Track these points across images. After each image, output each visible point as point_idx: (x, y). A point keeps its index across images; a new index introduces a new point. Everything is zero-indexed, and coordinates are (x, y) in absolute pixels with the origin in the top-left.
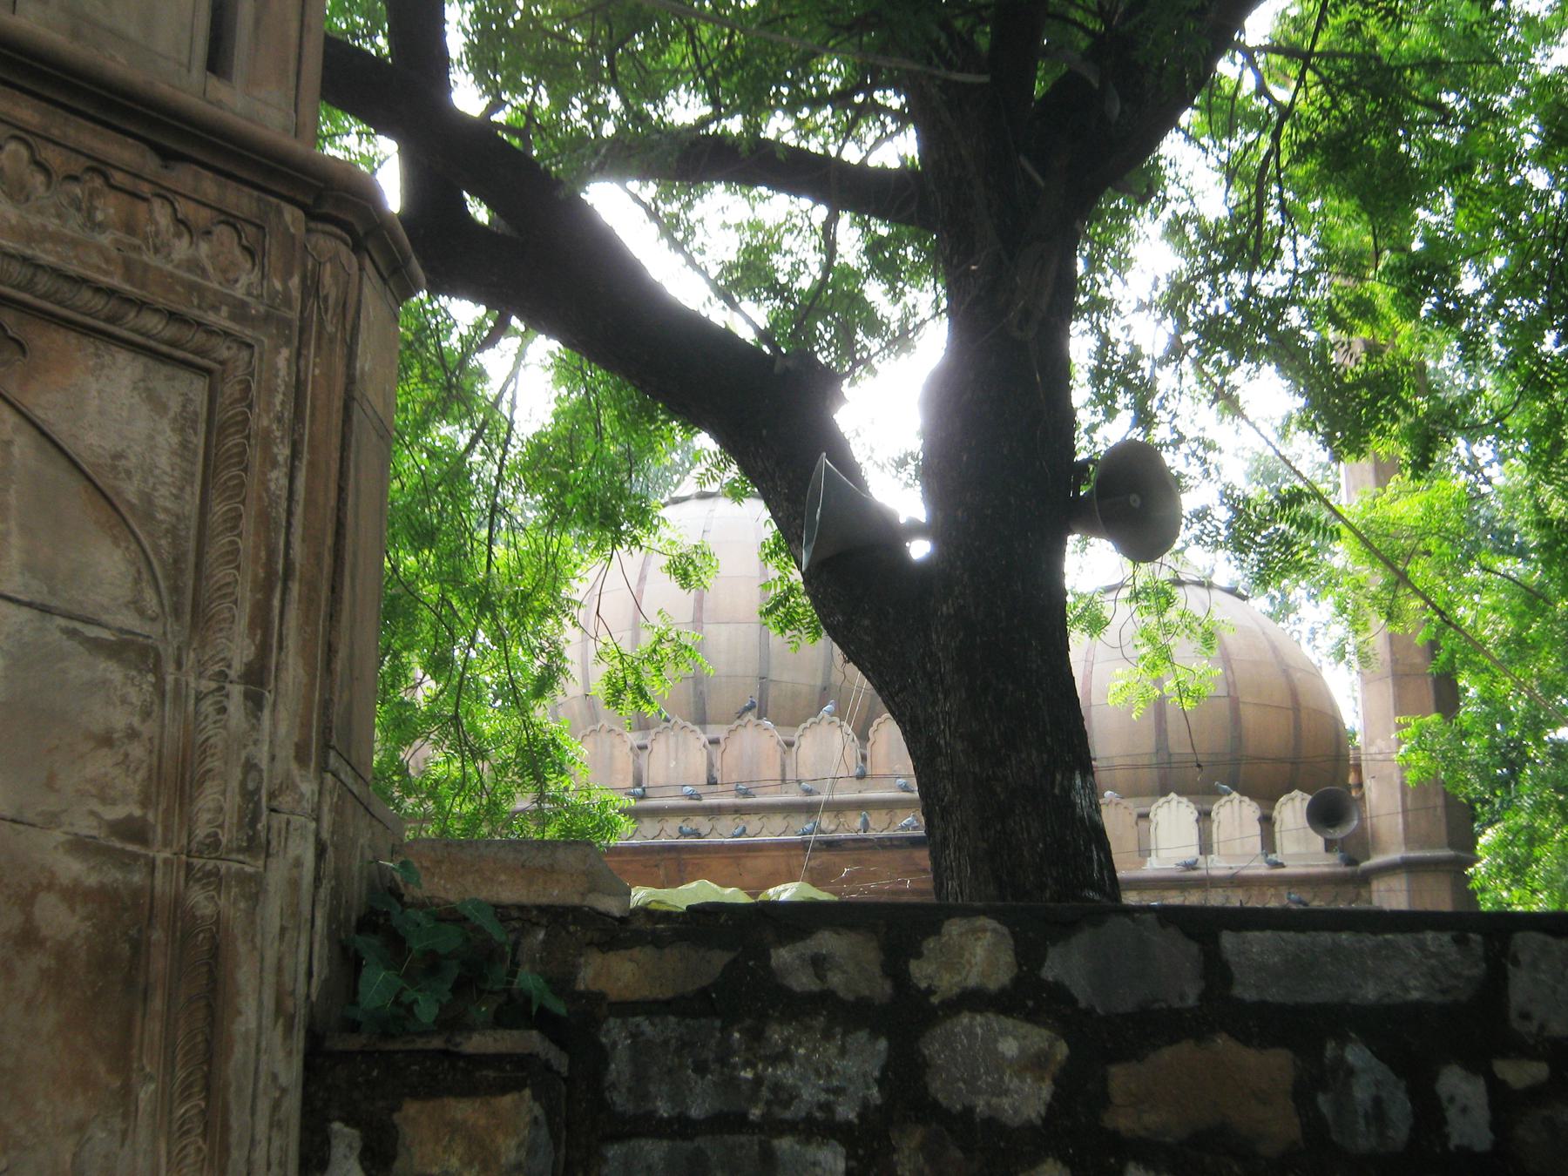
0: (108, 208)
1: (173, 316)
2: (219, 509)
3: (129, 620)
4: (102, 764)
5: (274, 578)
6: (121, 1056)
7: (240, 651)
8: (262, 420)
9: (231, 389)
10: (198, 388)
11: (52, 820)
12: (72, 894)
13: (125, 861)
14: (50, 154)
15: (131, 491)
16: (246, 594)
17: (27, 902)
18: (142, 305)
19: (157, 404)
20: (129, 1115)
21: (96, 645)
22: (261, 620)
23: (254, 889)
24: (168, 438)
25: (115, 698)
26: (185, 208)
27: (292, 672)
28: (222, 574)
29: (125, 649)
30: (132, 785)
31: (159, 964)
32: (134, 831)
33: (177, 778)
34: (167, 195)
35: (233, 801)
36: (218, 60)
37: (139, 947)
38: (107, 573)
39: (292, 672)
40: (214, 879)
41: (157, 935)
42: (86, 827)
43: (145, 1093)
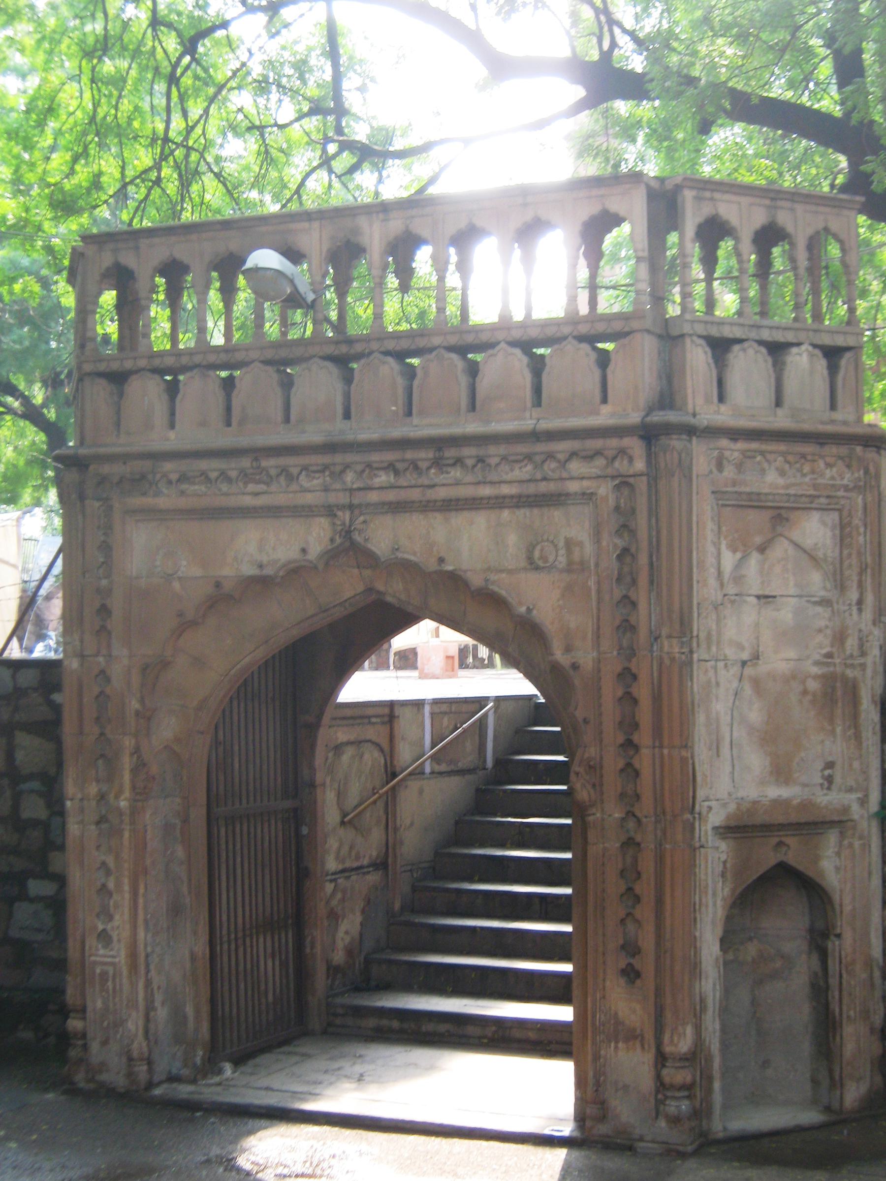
0: (806, 468)
1: (828, 497)
2: (845, 552)
3: (823, 593)
4: (819, 638)
5: (862, 572)
6: (831, 720)
7: (854, 595)
8: (856, 521)
9: (845, 513)
10: (835, 516)
11: (808, 657)
12: (816, 677)
13: (827, 664)
14: (790, 458)
15: (820, 554)
16: (855, 578)
17: (803, 682)
18: (819, 497)
19: (824, 524)
20: (835, 736)
21: (816, 603)
22: (860, 585)
23: (863, 666)
24: (829, 534)
25: (821, 617)
26: (828, 459)
27: (870, 599)
28: (847, 573)
29: (825, 602)
30: (827, 642)
31: (839, 693)
32: (829, 655)
33: (840, 638)
34: (822, 457)
35: (856, 642)
36: (833, 406)
37: (834, 689)
38: (816, 580)
39: (870, 599)
40: (852, 666)
41: (838, 684)
42: (817, 657)
43: (839, 730)
